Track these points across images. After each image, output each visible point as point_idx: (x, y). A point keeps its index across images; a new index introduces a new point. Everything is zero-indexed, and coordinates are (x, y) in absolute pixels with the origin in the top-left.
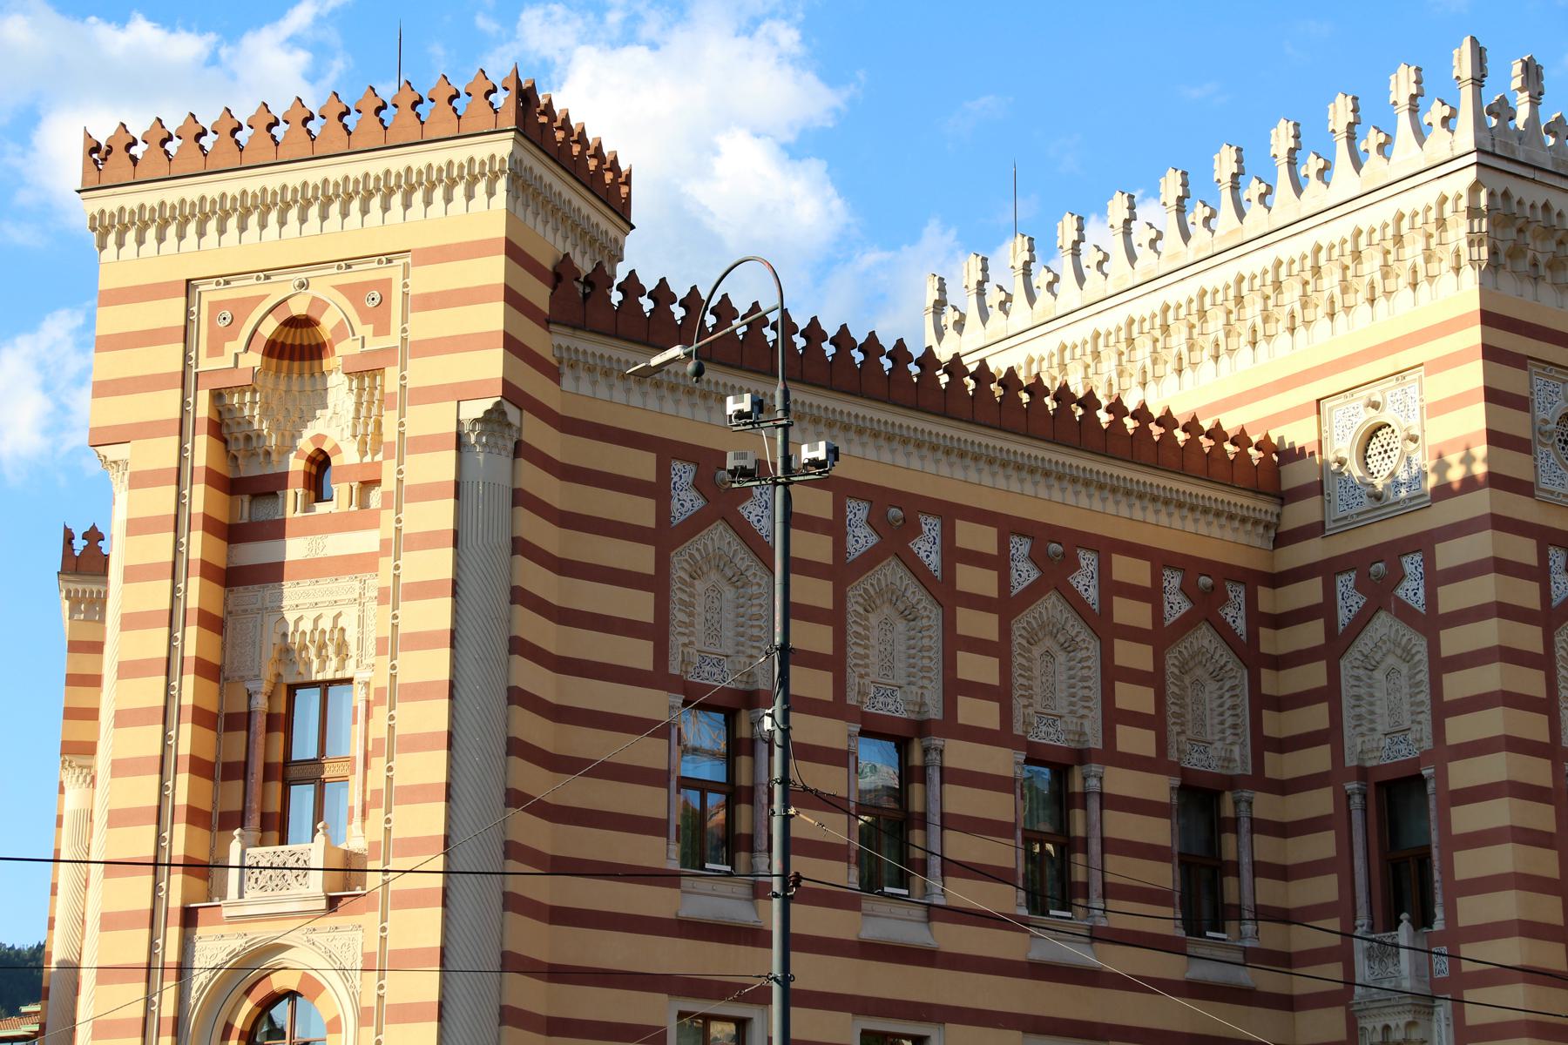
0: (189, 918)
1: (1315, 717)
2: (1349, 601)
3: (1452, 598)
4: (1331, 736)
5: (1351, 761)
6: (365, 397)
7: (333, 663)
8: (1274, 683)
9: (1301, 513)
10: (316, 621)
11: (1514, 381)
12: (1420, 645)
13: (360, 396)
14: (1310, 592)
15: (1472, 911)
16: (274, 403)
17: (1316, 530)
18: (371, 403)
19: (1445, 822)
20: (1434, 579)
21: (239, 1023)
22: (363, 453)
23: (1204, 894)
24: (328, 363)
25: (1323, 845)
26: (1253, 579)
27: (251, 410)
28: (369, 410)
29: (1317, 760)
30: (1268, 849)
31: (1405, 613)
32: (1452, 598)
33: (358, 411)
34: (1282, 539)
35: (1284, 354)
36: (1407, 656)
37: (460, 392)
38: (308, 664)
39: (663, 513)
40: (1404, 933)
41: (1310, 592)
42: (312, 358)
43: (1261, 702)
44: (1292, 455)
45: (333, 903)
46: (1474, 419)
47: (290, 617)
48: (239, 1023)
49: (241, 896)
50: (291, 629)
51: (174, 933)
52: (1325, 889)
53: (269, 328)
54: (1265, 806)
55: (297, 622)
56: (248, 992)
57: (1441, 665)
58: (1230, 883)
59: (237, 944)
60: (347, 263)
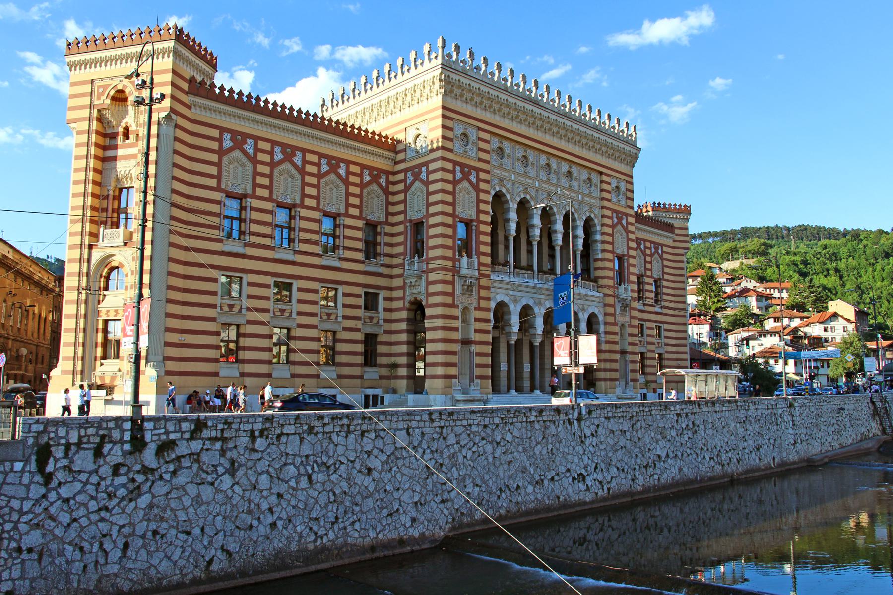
0: (90, 247)
1: (401, 207)
2: (410, 178)
3: (432, 177)
4: (404, 212)
5: (408, 218)
8: (392, 199)
9: (401, 156)
11: (449, 124)
12: (425, 189)
14: (401, 176)
15: (432, 254)
17: (404, 161)
19: (427, 232)
20: (429, 172)
23: (370, 250)
24: (129, 103)
25: (401, 239)
26: (388, 173)
27: (108, 115)
29: (401, 218)
30: (388, 239)
31: (422, 181)
32: (432, 177)
34: (396, 163)
35: (399, 116)
36: (422, 192)
39: (221, 145)
40: (416, 258)
41: (401, 176)
43: (388, 203)
44: (399, 142)
45: (125, 244)
46: (439, 133)
47: (118, 170)
52: (401, 249)
54: (388, 229)
58: (378, 247)
59: (102, 254)
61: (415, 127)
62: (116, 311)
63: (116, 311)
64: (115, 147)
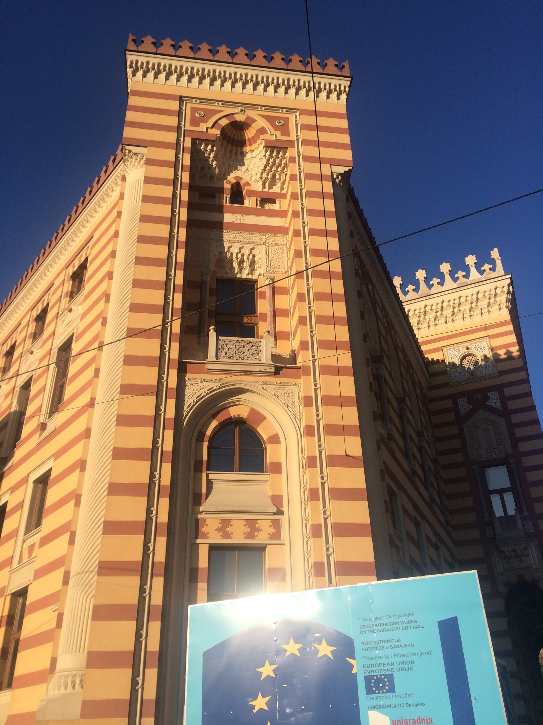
0: (182, 369)
1: (456, 443)
2: (464, 406)
6: (271, 161)
7: (247, 271)
9: (441, 379)
13: (269, 160)
14: (448, 403)
16: (219, 156)
18: (274, 164)
20: (504, 399)
21: (209, 432)
22: (264, 187)
24: (247, 149)
27: (210, 153)
28: (271, 167)
31: (492, 410)
33: (265, 167)
37: (333, 162)
38: (233, 268)
42: (237, 146)
47: (226, 245)
48: (209, 432)
49: (217, 358)
50: (226, 250)
51: (174, 374)
53: (224, 122)
55: (229, 248)
56: (214, 416)
57: (511, 427)
59: (215, 385)
60: (268, 108)
61: (465, 344)
62: (251, 523)
63: (251, 523)
64: (220, 209)
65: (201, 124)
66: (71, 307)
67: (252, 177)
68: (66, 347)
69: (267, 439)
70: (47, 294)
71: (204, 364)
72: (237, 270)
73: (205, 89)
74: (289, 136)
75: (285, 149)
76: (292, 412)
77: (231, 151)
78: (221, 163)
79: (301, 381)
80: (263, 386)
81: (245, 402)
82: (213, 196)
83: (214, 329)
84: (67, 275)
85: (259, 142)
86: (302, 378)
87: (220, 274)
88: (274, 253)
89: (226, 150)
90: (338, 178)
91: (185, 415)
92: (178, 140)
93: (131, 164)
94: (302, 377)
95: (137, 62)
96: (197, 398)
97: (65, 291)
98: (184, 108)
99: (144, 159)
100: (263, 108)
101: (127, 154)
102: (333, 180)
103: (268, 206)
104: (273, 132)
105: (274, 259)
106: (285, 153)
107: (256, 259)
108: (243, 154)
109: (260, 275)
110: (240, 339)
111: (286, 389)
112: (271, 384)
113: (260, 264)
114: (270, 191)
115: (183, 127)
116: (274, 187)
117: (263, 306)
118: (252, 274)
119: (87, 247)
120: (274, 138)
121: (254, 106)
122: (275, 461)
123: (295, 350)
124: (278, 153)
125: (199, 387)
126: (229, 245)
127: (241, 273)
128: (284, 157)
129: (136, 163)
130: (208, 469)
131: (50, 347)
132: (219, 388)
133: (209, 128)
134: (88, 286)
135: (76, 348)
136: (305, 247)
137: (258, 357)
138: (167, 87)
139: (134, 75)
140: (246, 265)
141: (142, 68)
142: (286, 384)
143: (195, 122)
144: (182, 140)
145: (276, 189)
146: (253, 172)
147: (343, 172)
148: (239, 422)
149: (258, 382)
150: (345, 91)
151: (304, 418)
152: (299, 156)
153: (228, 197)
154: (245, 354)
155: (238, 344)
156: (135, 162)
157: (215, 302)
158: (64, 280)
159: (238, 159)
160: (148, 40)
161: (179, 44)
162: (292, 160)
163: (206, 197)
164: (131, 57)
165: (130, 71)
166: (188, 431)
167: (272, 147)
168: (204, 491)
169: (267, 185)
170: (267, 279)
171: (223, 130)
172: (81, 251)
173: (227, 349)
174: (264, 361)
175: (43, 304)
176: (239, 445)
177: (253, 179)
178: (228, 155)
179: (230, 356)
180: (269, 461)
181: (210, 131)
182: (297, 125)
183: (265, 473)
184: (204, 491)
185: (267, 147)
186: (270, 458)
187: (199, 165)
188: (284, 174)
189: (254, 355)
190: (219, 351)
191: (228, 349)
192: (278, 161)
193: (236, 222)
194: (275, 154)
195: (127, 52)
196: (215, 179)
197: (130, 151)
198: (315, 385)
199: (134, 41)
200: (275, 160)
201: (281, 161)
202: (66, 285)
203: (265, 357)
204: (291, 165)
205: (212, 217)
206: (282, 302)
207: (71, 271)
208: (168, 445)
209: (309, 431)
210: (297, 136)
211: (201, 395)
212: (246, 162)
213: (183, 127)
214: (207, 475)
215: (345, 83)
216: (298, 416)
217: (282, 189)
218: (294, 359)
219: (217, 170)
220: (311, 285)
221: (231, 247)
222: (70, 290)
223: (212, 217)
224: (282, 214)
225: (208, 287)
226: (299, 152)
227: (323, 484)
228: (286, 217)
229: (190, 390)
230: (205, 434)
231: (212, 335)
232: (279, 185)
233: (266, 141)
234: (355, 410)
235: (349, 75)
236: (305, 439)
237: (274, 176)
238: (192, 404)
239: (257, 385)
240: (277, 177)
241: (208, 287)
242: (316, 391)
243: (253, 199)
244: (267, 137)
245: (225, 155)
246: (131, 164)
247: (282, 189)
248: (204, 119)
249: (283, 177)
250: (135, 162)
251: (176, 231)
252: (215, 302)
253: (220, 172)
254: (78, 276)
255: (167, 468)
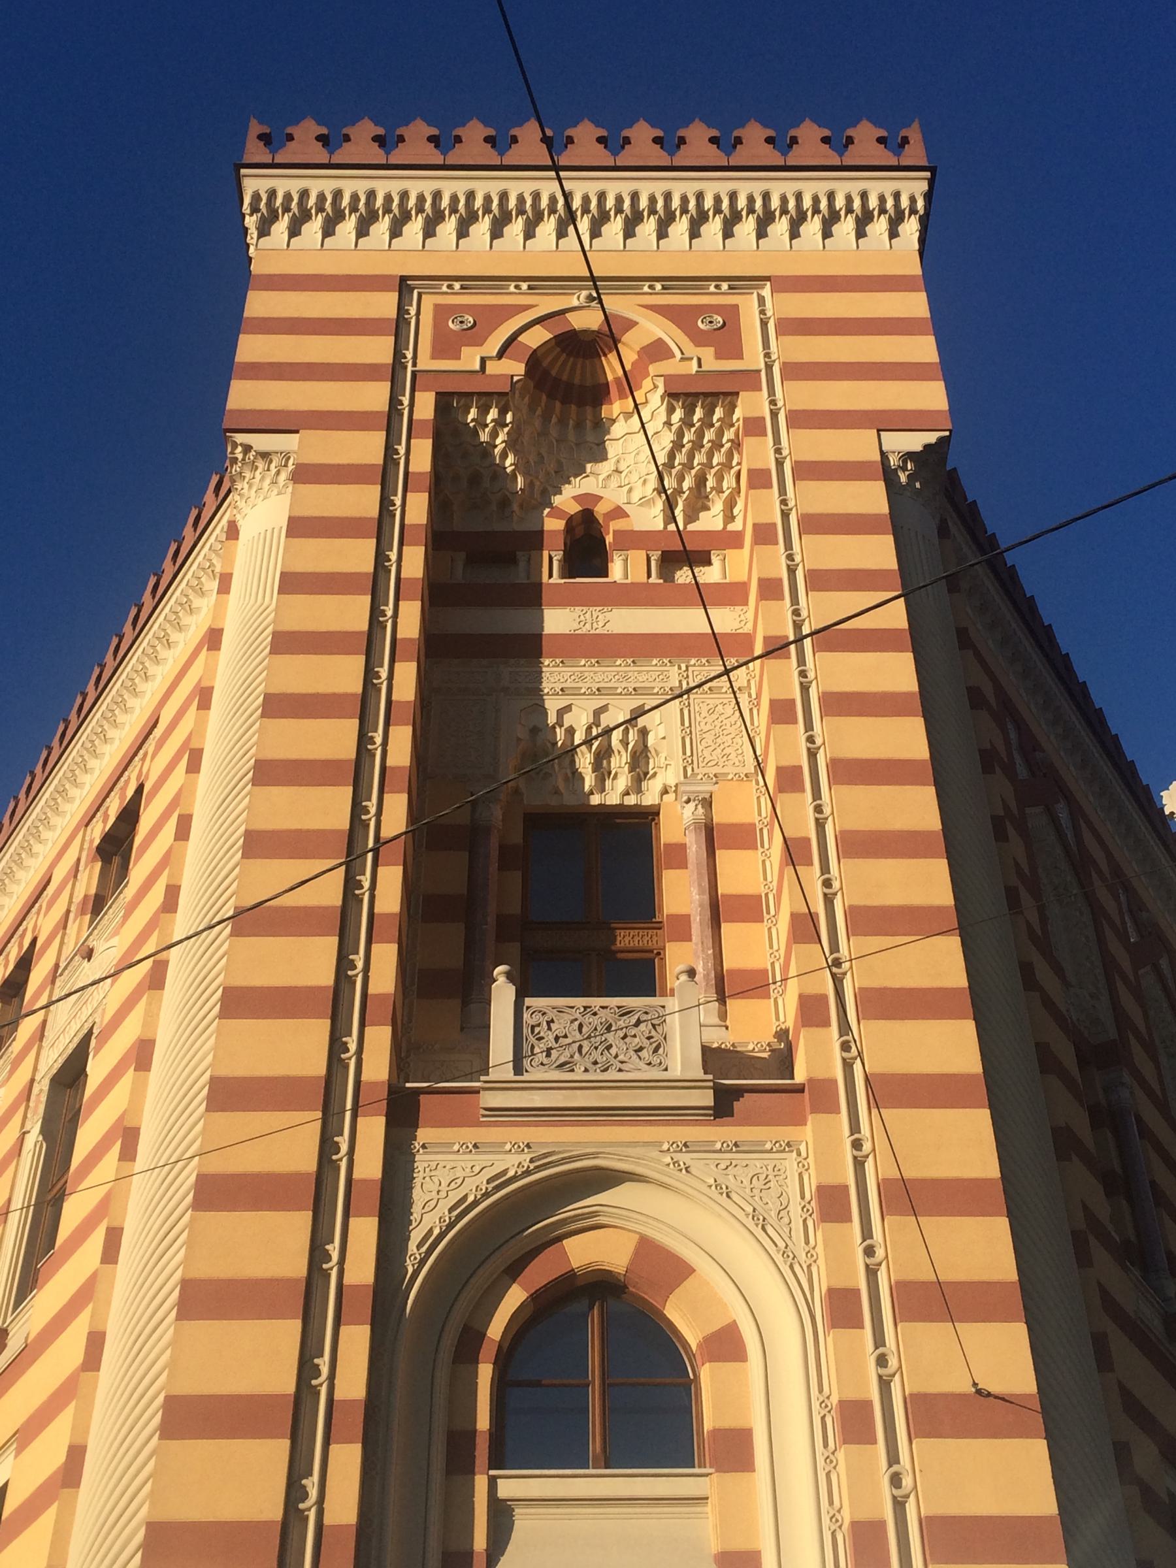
0: (403, 1114)
6: (688, 436)
7: (623, 781)
10: (598, 713)
13: (680, 434)
16: (526, 439)
18: (698, 445)
21: (496, 1329)
27: (495, 431)
28: (691, 456)
38: (579, 778)
42: (581, 404)
47: (552, 705)
48: (496, 1329)
49: (518, 1069)
50: (552, 719)
51: (372, 1131)
53: (537, 338)
55: (561, 713)
56: (513, 1272)
59: (512, 1163)
60: (670, 283)
64: (532, 597)
65: (466, 351)
66: (90, 943)
67: (630, 491)
68: (71, 1075)
69: (699, 1346)
70: (34, 910)
71: (476, 1091)
72: (589, 781)
73: (479, 249)
74: (740, 356)
75: (730, 398)
76: (781, 1245)
77: (563, 422)
78: (532, 459)
79: (807, 1134)
80: (677, 1156)
81: (606, 1214)
82: (512, 560)
83: (509, 976)
84: (86, 846)
85: (647, 384)
86: (809, 1123)
87: (537, 799)
88: (709, 720)
89: (546, 417)
90: (904, 469)
91: (410, 1270)
92: (394, 401)
93: (250, 486)
94: (810, 1118)
95: (272, 194)
96: (451, 1210)
97: (79, 897)
98: (413, 311)
99: (291, 467)
100: (658, 286)
101: (240, 457)
102: (888, 476)
103: (683, 576)
104: (691, 349)
105: (709, 738)
106: (731, 409)
107: (651, 740)
108: (601, 427)
109: (665, 791)
110: (596, 1002)
111: (756, 1163)
112: (706, 1148)
113: (663, 755)
114: (691, 527)
115: (410, 365)
116: (702, 515)
117: (679, 892)
118: (639, 791)
119: (141, 752)
120: (694, 367)
121: (627, 283)
122: (728, 1423)
123: (787, 1031)
124: (710, 412)
125: (460, 1174)
126: (562, 703)
127: (603, 790)
128: (727, 422)
129: (268, 481)
130: (498, 1460)
131: (29, 1077)
132: (528, 1173)
133: (491, 358)
134: (139, 872)
135: (97, 1069)
136: (805, 689)
137: (656, 1060)
138: (363, 262)
139: (264, 231)
140: (620, 762)
141: (287, 209)
142: (756, 1148)
143: (446, 346)
144: (406, 401)
145: (711, 520)
146: (634, 477)
147: (919, 448)
148: (601, 1287)
149: (661, 1143)
150: (913, 211)
151: (821, 1262)
152: (774, 415)
153: (558, 556)
154: (613, 1051)
155: (588, 1019)
156: (262, 479)
157: (512, 881)
158: (79, 860)
159: (590, 444)
160: (307, 131)
161: (398, 132)
162: (754, 426)
163: (483, 559)
164: (254, 184)
165: (251, 222)
166: (421, 1327)
167: (687, 395)
168: (480, 1542)
169: (679, 512)
170: (688, 801)
171: (534, 361)
172: (125, 769)
173: (551, 1037)
174: (676, 1071)
175: (21, 946)
176: (606, 1374)
177: (635, 496)
178: (554, 432)
179: (562, 1060)
180: (708, 1425)
181: (493, 368)
182: (764, 324)
183: (696, 1470)
184: (480, 1542)
185: (672, 396)
186: (712, 1415)
187: (460, 468)
188: (733, 471)
189: (644, 1054)
190: (526, 1048)
191: (557, 1039)
192: (709, 435)
193: (584, 631)
194: (699, 413)
195: (243, 171)
196: (515, 507)
197: (247, 448)
198: (857, 1145)
199: (265, 138)
200: (700, 435)
201: (720, 433)
202: (83, 876)
203: (682, 1058)
204: (748, 443)
205: (509, 621)
206: (740, 872)
207: (97, 831)
208: (352, 1380)
209: (842, 1308)
210: (767, 355)
211: (465, 1197)
212: (612, 449)
213: (410, 365)
214: (492, 1482)
215: (914, 187)
216: (802, 1257)
217: (729, 517)
218: (783, 1060)
219: (520, 479)
220: (827, 810)
221: (568, 708)
222: (93, 891)
223: (509, 621)
224: (733, 594)
225: (494, 842)
226: (773, 402)
227: (899, 1505)
228: (745, 603)
229: (430, 1185)
230: (482, 1335)
231: (503, 994)
232: (717, 506)
233: (668, 379)
234: (1001, 1226)
235: (924, 163)
236: (830, 1339)
237: (701, 480)
238: (436, 1231)
239: (655, 1154)
240: (710, 483)
241: (494, 842)
242: (859, 1164)
243: (638, 557)
244: (672, 367)
245: (544, 433)
246: (250, 486)
247: (729, 517)
248: (475, 334)
249: (728, 482)
250: (262, 479)
251: (384, 673)
252: (512, 881)
253: (530, 485)
254: (116, 848)
255: (346, 1462)
